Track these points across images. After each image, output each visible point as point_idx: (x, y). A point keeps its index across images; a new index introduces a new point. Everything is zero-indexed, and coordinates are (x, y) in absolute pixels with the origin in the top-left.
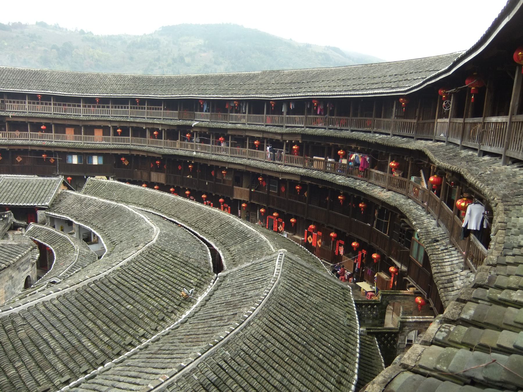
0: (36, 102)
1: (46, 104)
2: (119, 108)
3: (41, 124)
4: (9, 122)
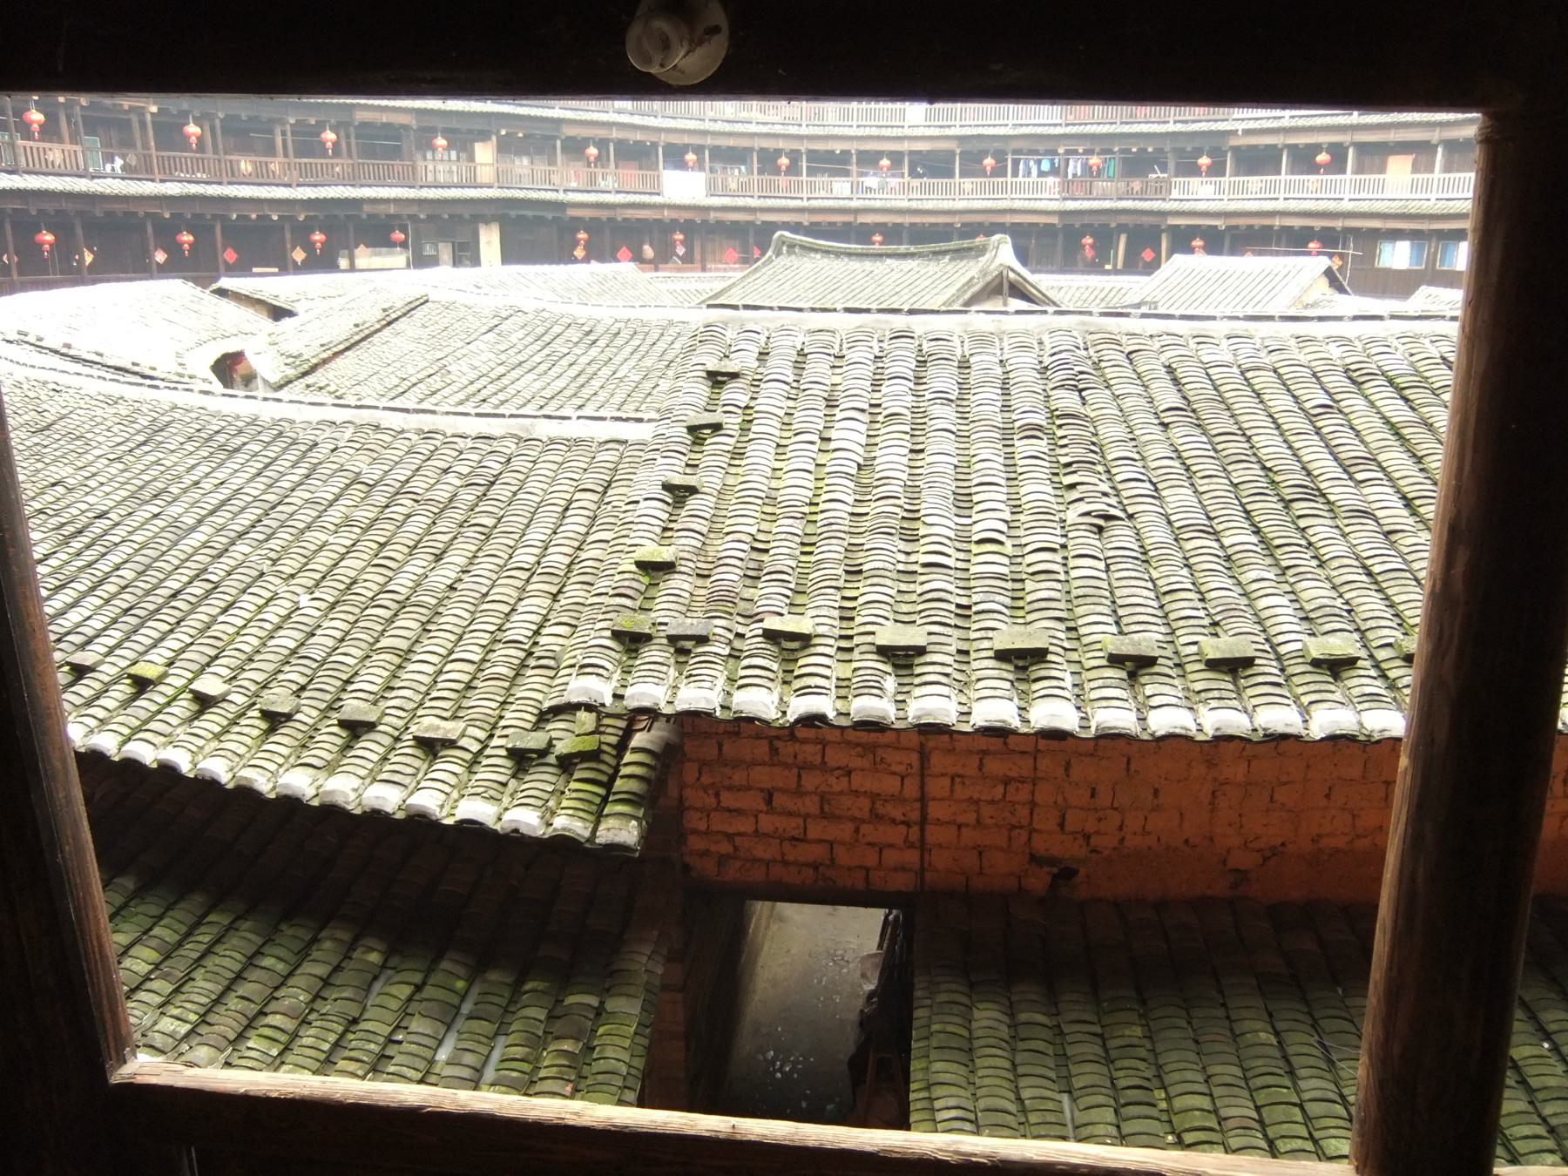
3: (1316, 148)
4: (1236, 149)
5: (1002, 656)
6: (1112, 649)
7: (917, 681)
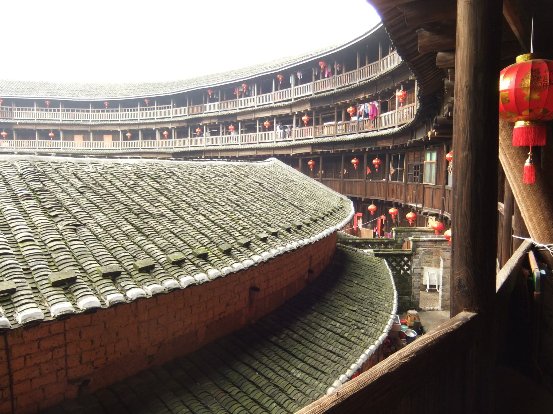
0: (44, 108)
1: (54, 110)
2: (128, 111)
3: (49, 131)
4: (17, 130)
5: (55, 284)
6: (103, 271)
7: (16, 305)
